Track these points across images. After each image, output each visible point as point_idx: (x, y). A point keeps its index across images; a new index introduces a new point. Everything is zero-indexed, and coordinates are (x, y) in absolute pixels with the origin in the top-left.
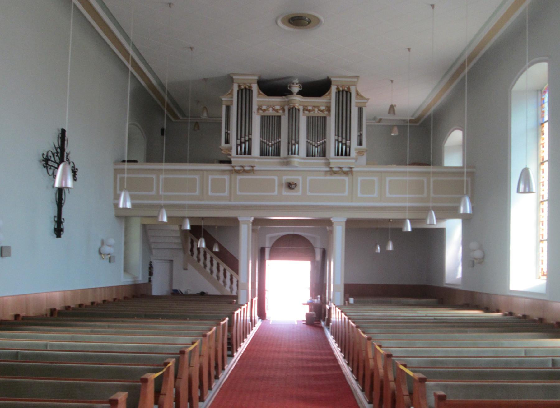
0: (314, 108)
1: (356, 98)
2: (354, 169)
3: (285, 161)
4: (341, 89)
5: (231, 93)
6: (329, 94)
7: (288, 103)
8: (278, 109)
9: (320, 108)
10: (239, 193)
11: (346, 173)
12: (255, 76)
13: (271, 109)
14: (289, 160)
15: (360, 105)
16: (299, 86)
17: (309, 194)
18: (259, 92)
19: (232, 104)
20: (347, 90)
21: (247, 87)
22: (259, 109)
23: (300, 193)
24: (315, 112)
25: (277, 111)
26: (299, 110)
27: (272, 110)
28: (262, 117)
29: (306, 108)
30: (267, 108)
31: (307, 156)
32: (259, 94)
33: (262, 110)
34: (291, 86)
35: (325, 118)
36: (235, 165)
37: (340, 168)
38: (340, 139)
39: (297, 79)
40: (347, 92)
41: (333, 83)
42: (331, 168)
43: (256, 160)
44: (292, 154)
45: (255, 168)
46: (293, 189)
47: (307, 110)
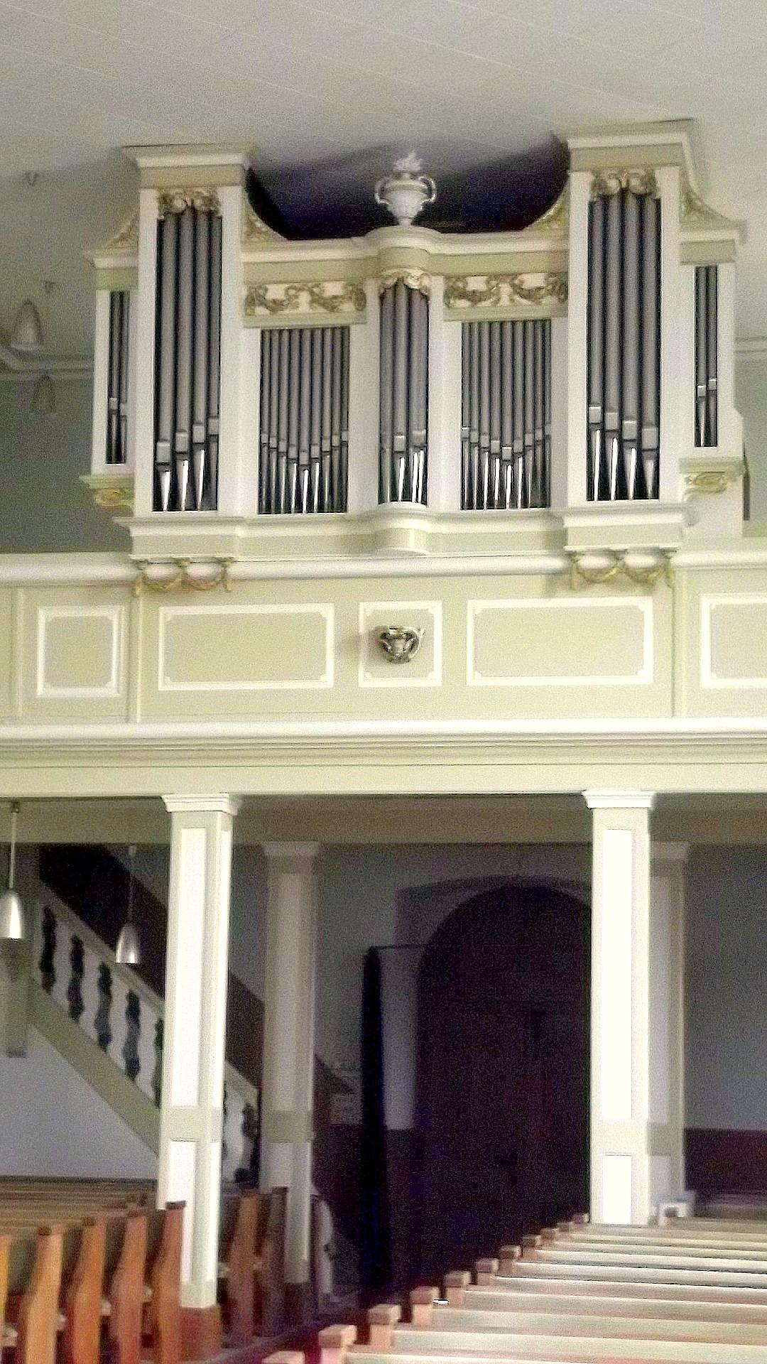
0: (494, 283)
1: (684, 223)
2: (676, 560)
3: (366, 530)
4: (613, 186)
5: (131, 237)
6: (559, 211)
7: (377, 264)
8: (335, 297)
9: (522, 282)
10: (165, 685)
11: (642, 580)
12: (227, 151)
13: (304, 298)
14: (380, 526)
15: (705, 258)
16: (426, 187)
18: (250, 224)
19: (135, 284)
21: (198, 203)
22: (254, 299)
23: (435, 679)
24: (499, 299)
25: (330, 304)
26: (426, 298)
27: (312, 302)
28: (268, 339)
29: (460, 285)
30: (289, 298)
31: (467, 504)
32: (251, 230)
33: (263, 303)
34: (388, 186)
35: (543, 325)
36: (148, 557)
37: (615, 555)
38: (612, 420)
39: (412, 156)
40: (641, 199)
41: (574, 163)
42: (571, 555)
43: (240, 532)
44: (394, 498)
45: (234, 570)
46: (403, 659)
47: (463, 295)
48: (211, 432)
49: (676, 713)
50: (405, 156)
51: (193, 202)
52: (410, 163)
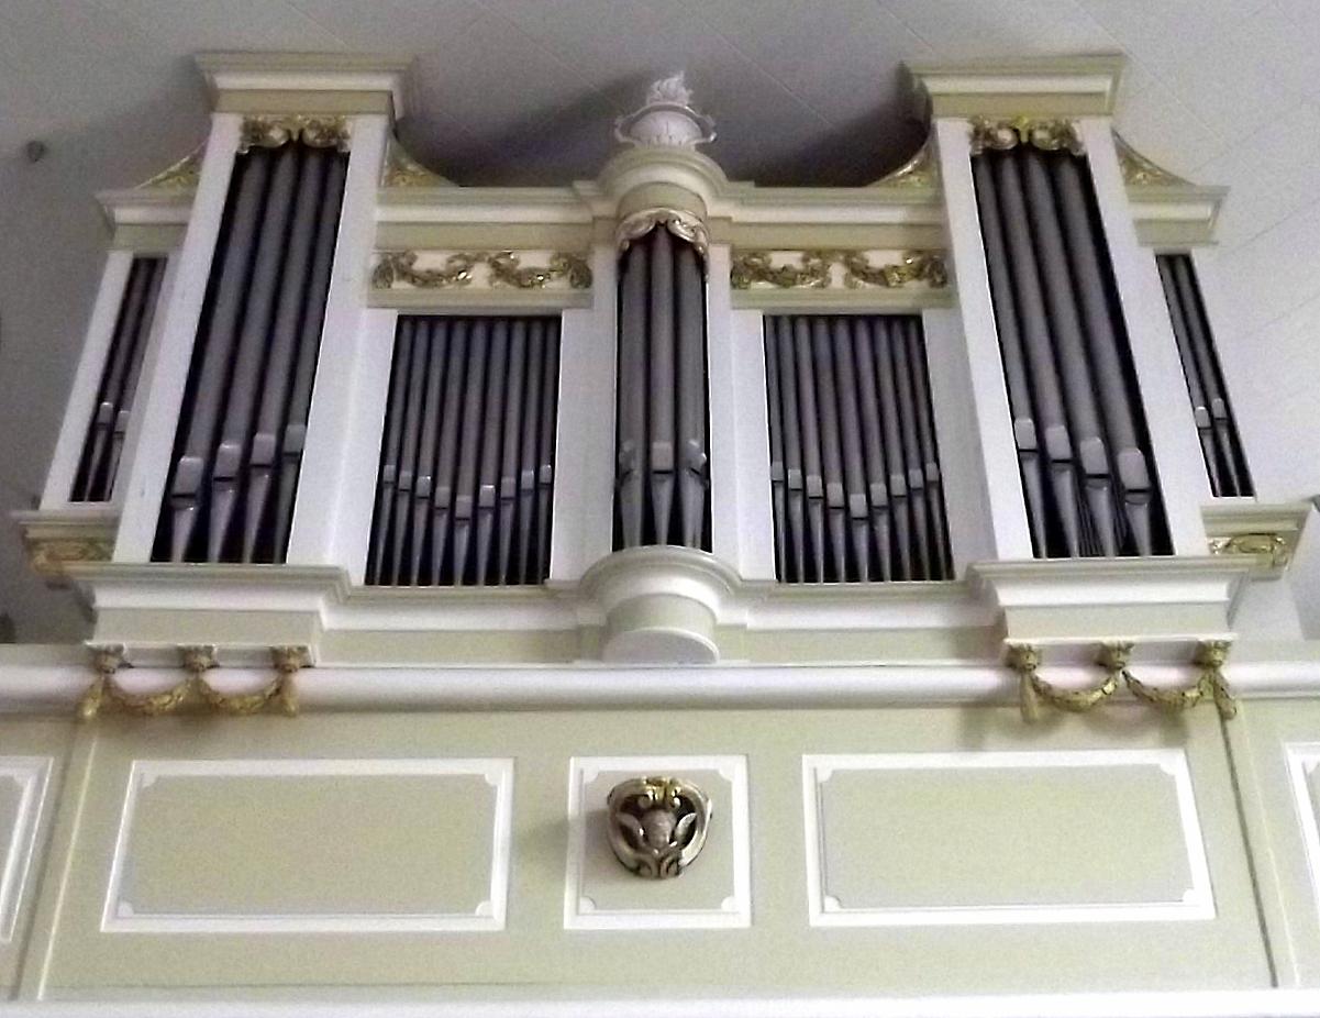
2: (1234, 673)
3: (588, 616)
8: (532, 272)
17: (825, 915)
20: (1054, 145)
22: (391, 268)
23: (735, 912)
45: (303, 682)
46: (667, 866)
47: (763, 274)
48: (287, 448)
49: (1279, 980)
50: (666, 75)
51: (301, 133)
52: (674, 86)
